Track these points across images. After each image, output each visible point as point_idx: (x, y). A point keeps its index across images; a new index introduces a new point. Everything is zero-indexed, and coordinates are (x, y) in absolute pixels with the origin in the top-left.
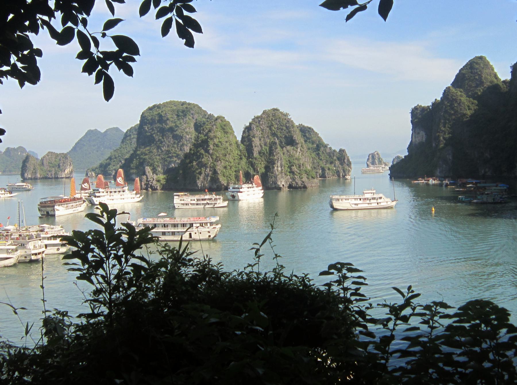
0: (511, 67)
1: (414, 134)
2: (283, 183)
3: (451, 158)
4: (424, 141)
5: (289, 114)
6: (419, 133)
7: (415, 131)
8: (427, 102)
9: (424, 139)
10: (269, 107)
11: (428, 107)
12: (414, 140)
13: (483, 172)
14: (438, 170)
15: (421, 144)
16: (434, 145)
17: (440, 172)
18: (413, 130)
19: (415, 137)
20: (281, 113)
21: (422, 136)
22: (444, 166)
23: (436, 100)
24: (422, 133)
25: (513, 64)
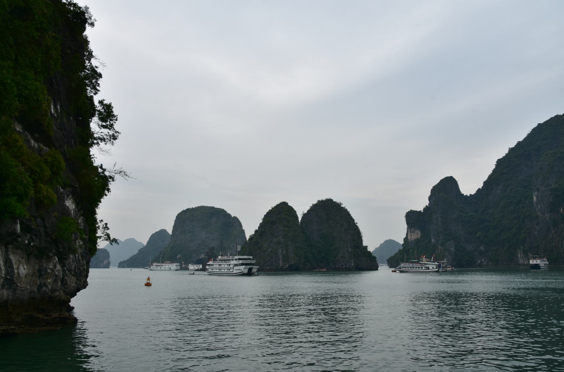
3: (453, 250)
5: (342, 204)
6: (414, 232)
7: (410, 230)
9: (419, 237)
10: (324, 197)
11: (420, 211)
12: (409, 237)
13: (479, 262)
15: (417, 241)
16: (433, 240)
18: (409, 230)
19: (411, 236)
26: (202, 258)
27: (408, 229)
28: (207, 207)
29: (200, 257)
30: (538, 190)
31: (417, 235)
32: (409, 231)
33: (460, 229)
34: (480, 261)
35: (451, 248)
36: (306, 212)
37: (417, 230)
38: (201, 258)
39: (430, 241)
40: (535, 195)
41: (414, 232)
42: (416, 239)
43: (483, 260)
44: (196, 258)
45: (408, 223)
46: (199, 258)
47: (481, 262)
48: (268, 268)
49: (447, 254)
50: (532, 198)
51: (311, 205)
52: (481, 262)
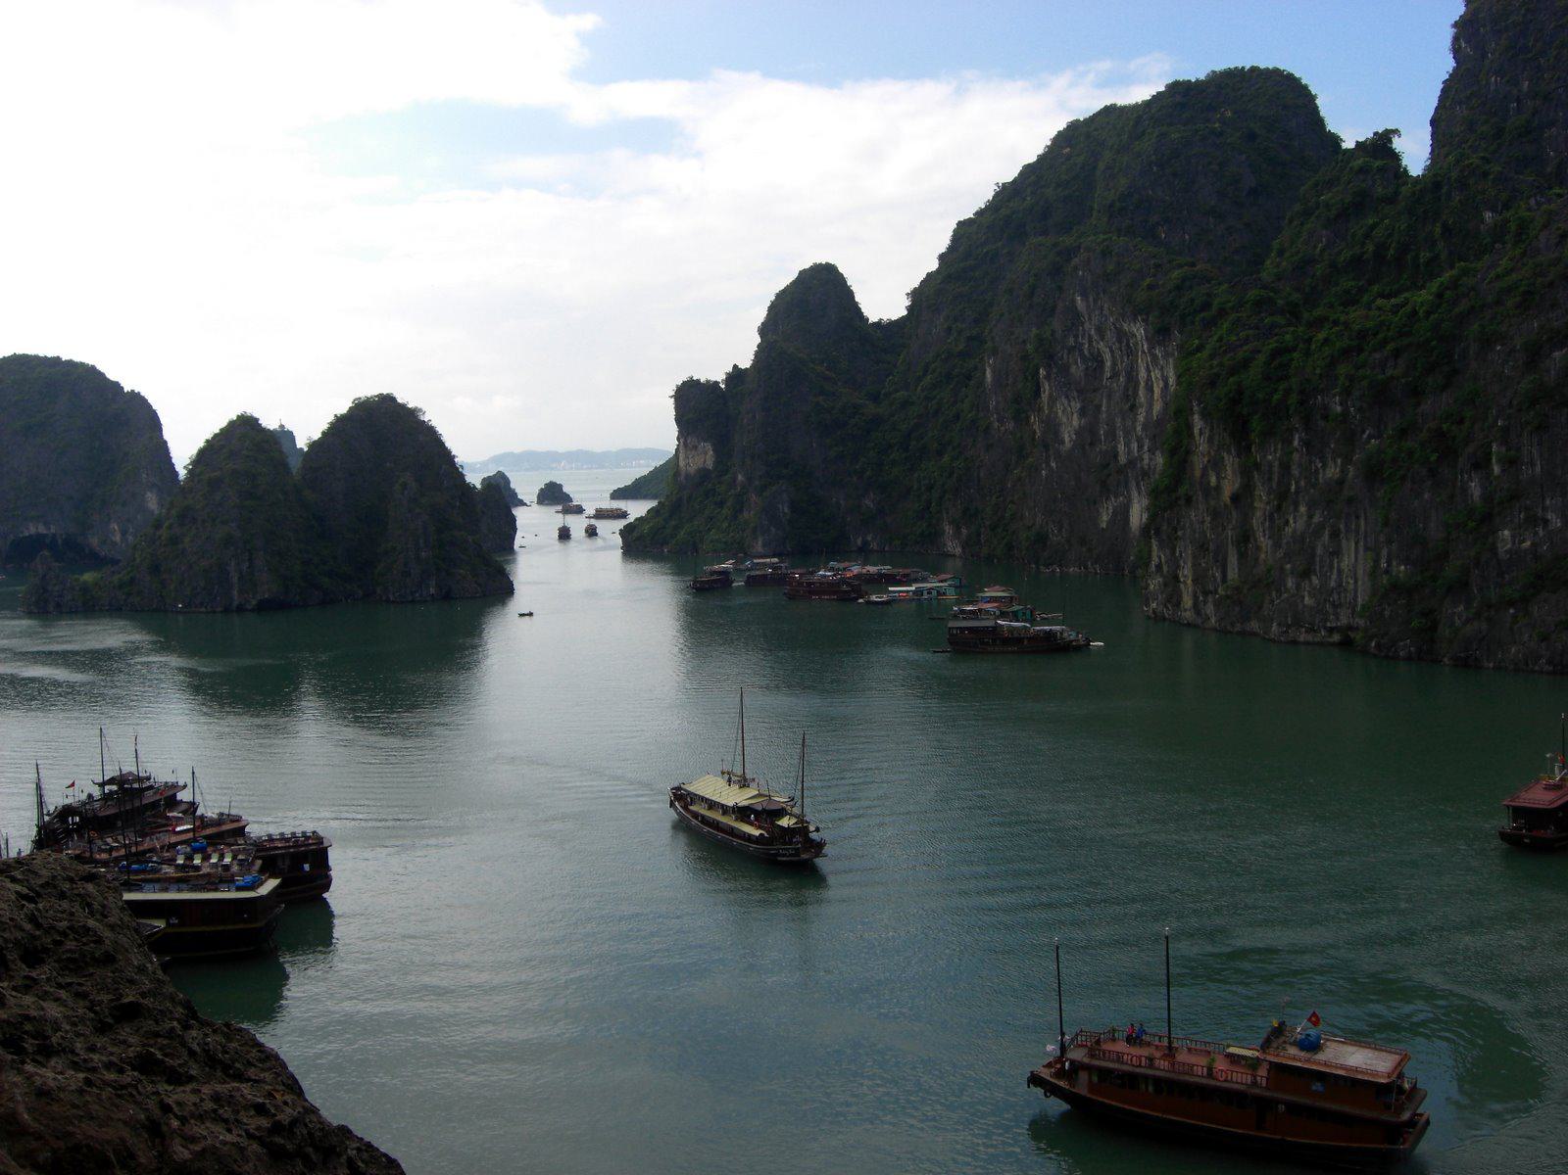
0: (908, 294)
2: (432, 591)
3: (786, 510)
6: (695, 448)
7: (686, 440)
8: (715, 372)
9: (710, 464)
12: (682, 463)
13: (859, 542)
15: (704, 475)
16: (740, 477)
17: (764, 546)
20: (403, 407)
21: (705, 457)
22: (773, 529)
23: (735, 367)
26: (31, 536)
27: (678, 439)
28: (36, 357)
29: (22, 532)
30: (995, 352)
31: (705, 457)
32: (682, 444)
35: (780, 506)
36: (317, 436)
38: (27, 534)
39: (735, 479)
40: (990, 365)
41: (695, 448)
42: (699, 471)
44: (12, 537)
45: (679, 420)
46: (21, 536)
47: (865, 543)
48: (203, 609)
50: (984, 373)
51: (331, 418)
52: (865, 543)
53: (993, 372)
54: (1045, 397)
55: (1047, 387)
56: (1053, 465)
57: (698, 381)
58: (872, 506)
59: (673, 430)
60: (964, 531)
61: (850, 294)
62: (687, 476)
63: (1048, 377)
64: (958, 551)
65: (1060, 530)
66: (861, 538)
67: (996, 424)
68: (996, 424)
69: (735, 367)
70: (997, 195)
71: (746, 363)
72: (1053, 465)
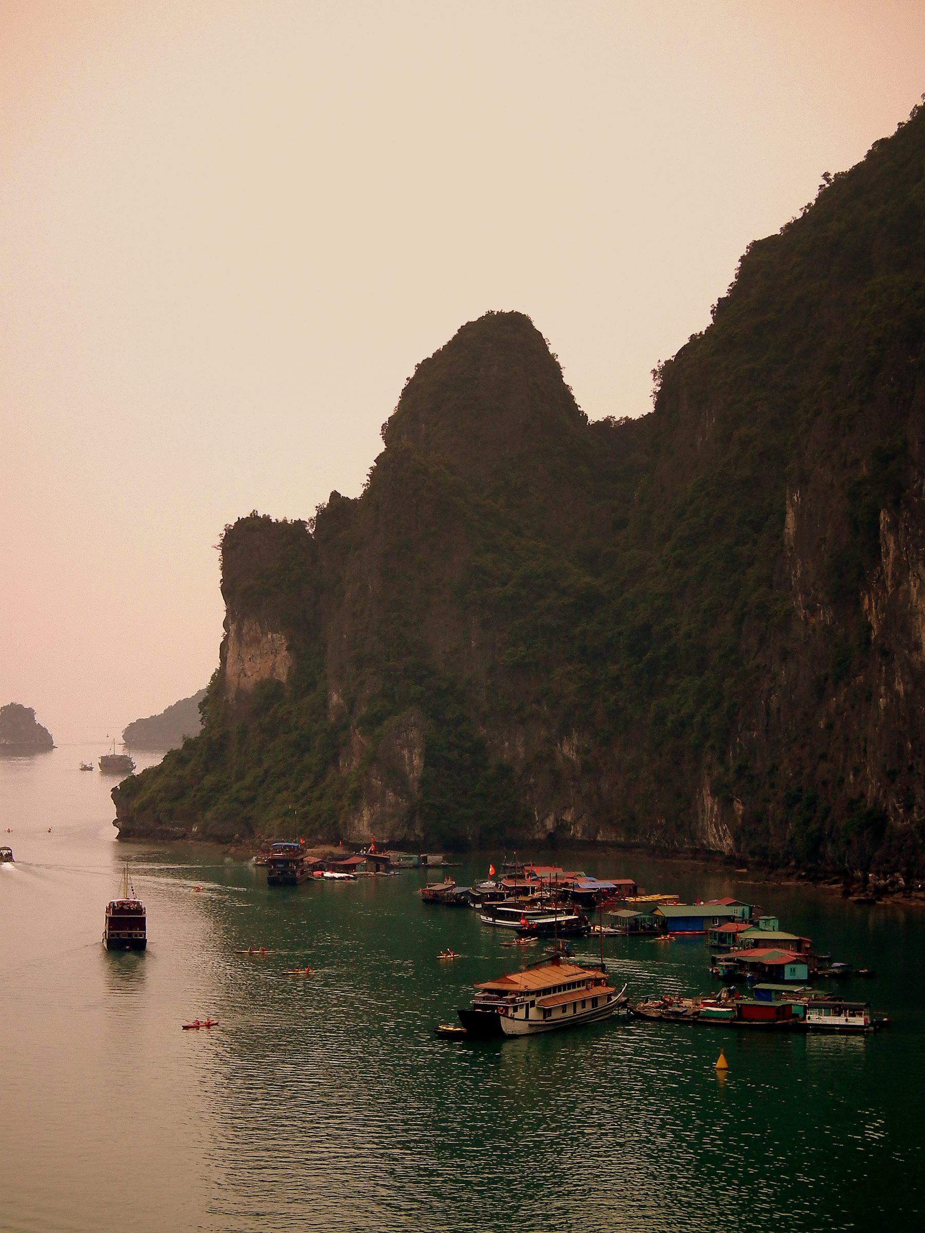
1: (230, 644)
3: (416, 762)
4: (284, 679)
6: (257, 640)
11: (300, 524)
12: (229, 671)
13: (550, 823)
14: (366, 814)
16: (335, 698)
17: (371, 825)
18: (232, 627)
19: (240, 659)
22: (390, 796)
23: (335, 495)
24: (279, 640)
25: (662, 363)
27: (226, 625)
33: (474, 644)
34: (556, 820)
35: (405, 752)
37: (275, 631)
41: (257, 640)
42: (261, 685)
43: (568, 817)
45: (227, 590)
47: (561, 826)
49: (377, 783)
52: (561, 826)
53: (799, 517)
54: (888, 563)
55: (892, 546)
56: (900, 687)
57: (267, 519)
58: (574, 756)
59: (218, 608)
60: (739, 807)
61: (553, 368)
62: (240, 691)
63: (894, 526)
64: (727, 844)
65: (909, 808)
66: (552, 818)
67: (802, 613)
68: (802, 613)
69: (335, 495)
70: (825, 195)
71: (354, 489)
72: (900, 687)
